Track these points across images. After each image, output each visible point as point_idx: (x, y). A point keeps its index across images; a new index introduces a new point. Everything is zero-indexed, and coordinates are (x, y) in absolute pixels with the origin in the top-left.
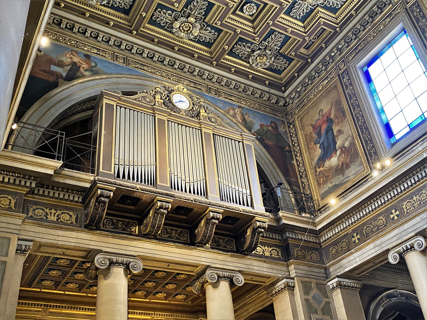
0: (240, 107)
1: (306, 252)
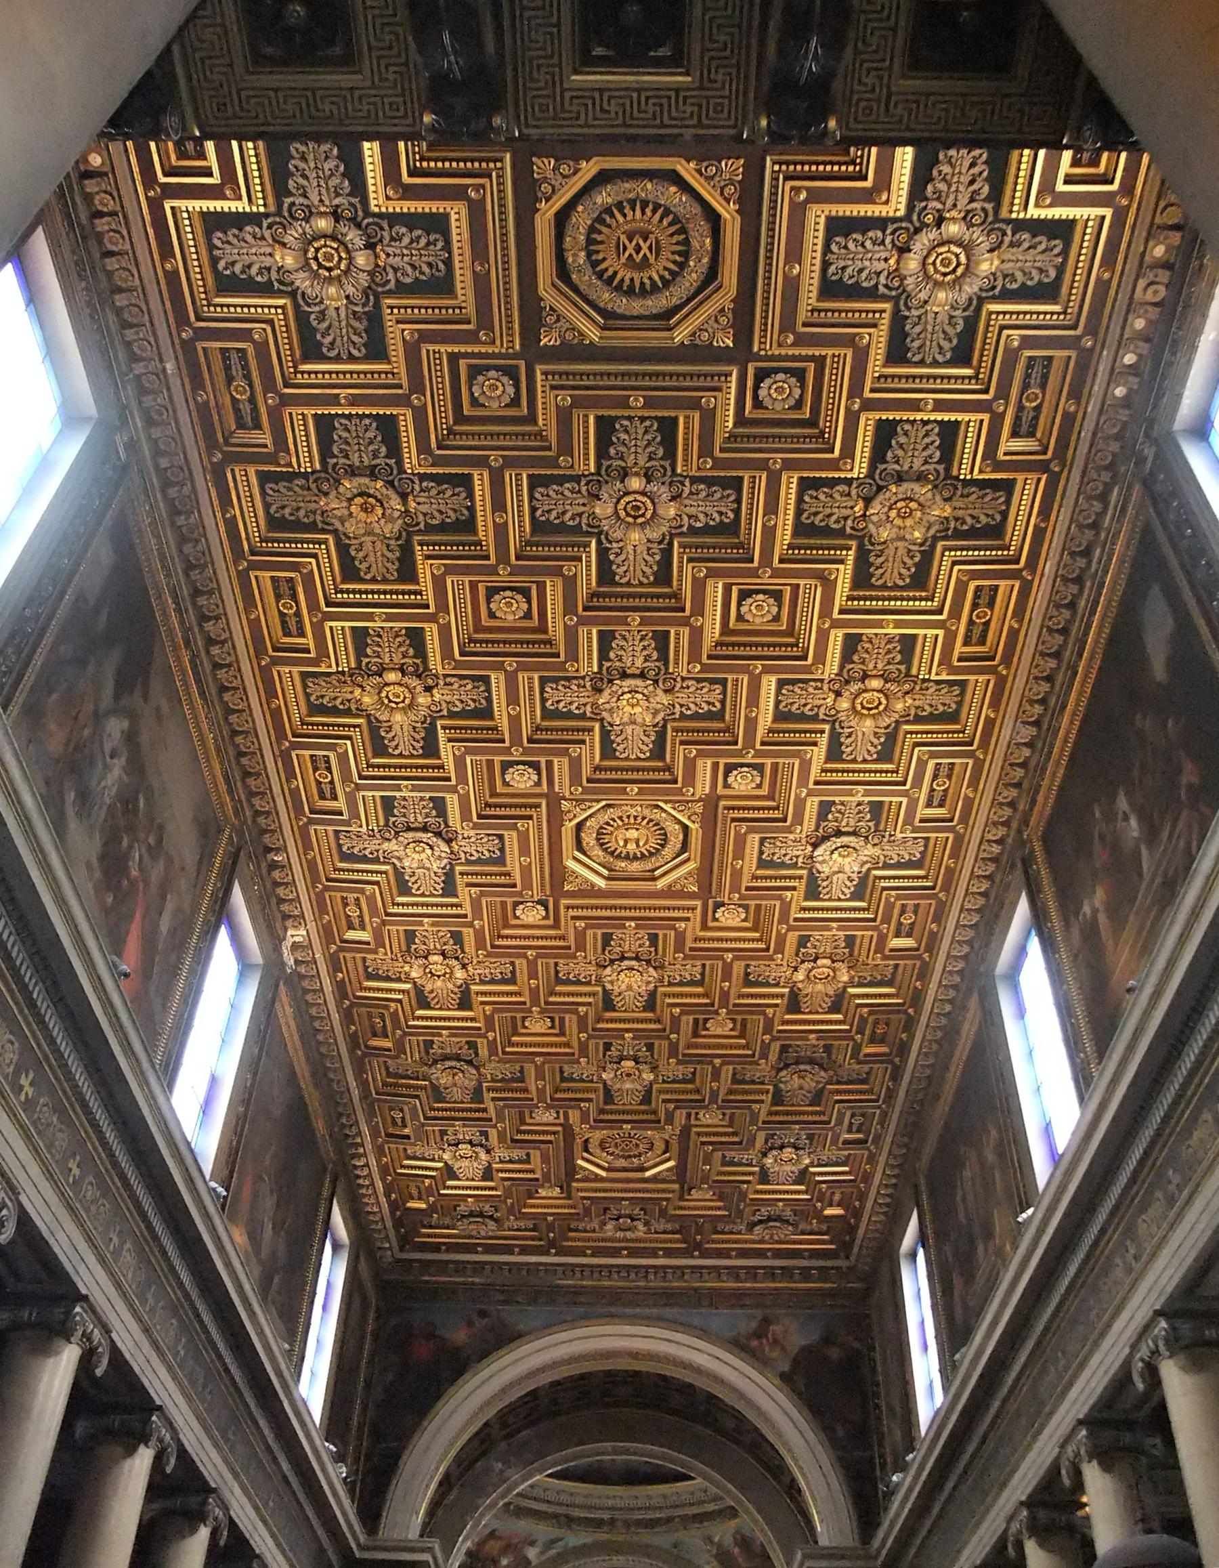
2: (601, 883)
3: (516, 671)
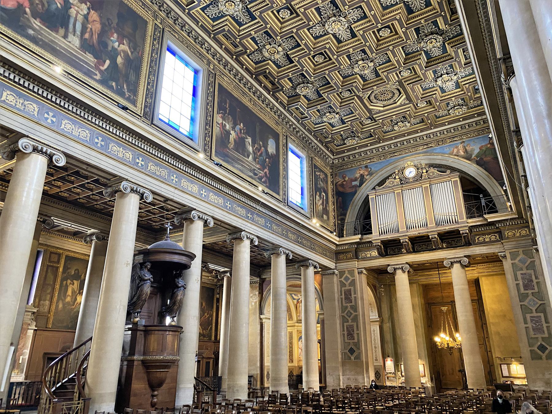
0: (461, 143)
1: (516, 230)
2: (382, 109)
3: (329, 73)
